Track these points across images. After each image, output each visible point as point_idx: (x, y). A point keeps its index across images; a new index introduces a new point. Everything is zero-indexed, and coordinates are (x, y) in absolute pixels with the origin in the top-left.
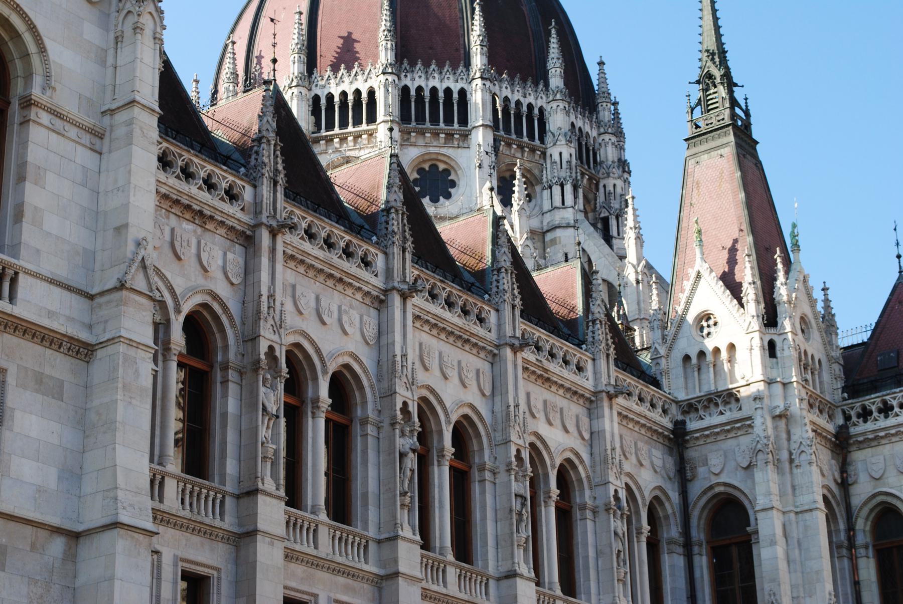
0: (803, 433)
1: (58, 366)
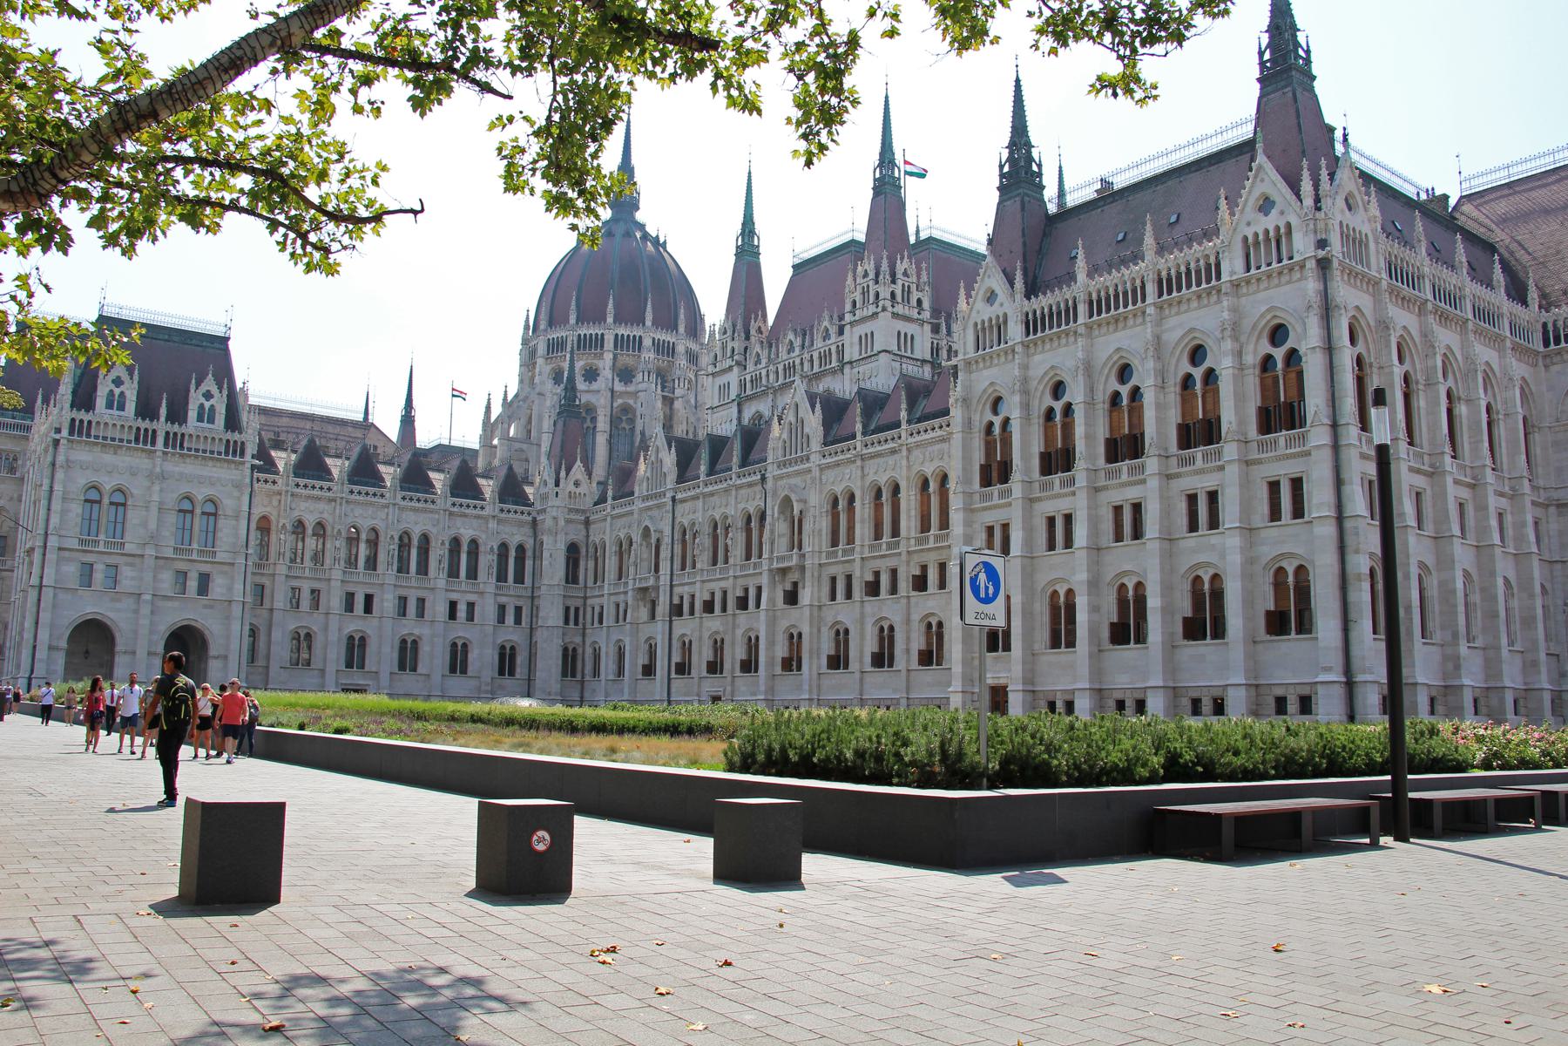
0: (562, 523)
1: (226, 568)
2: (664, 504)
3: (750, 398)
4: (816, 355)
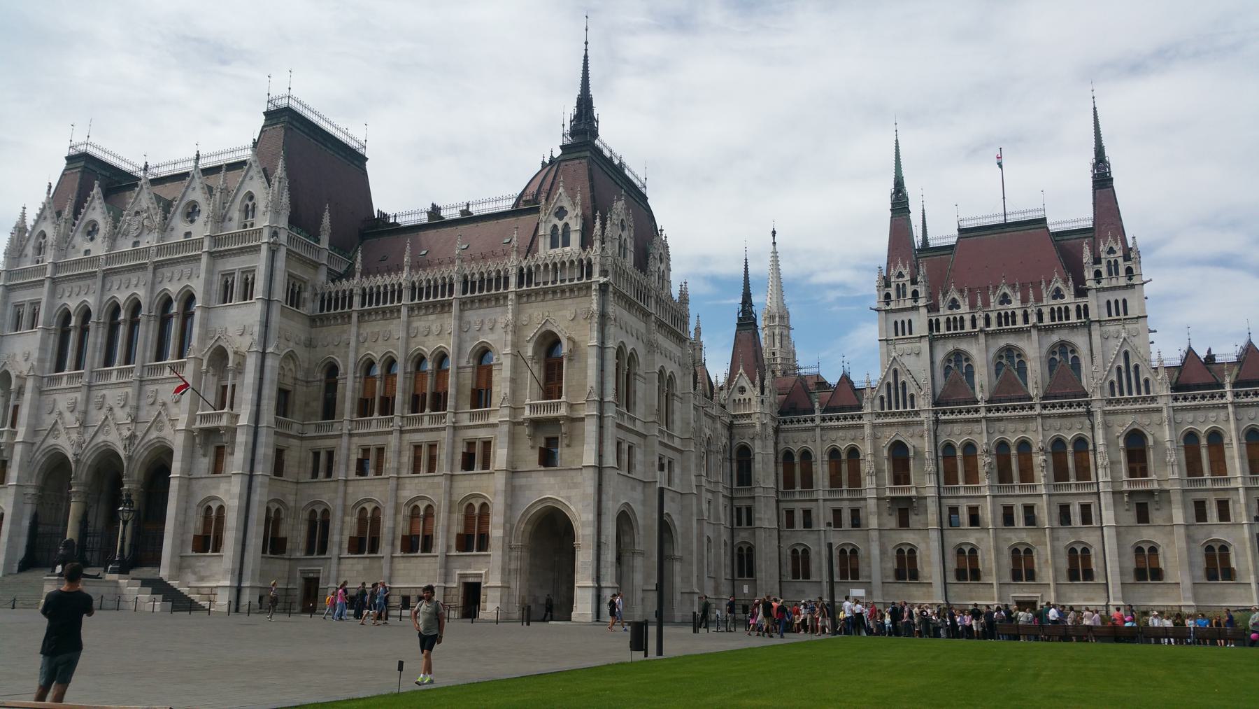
2: (922, 423)
3: (945, 337)
4: (1046, 311)
